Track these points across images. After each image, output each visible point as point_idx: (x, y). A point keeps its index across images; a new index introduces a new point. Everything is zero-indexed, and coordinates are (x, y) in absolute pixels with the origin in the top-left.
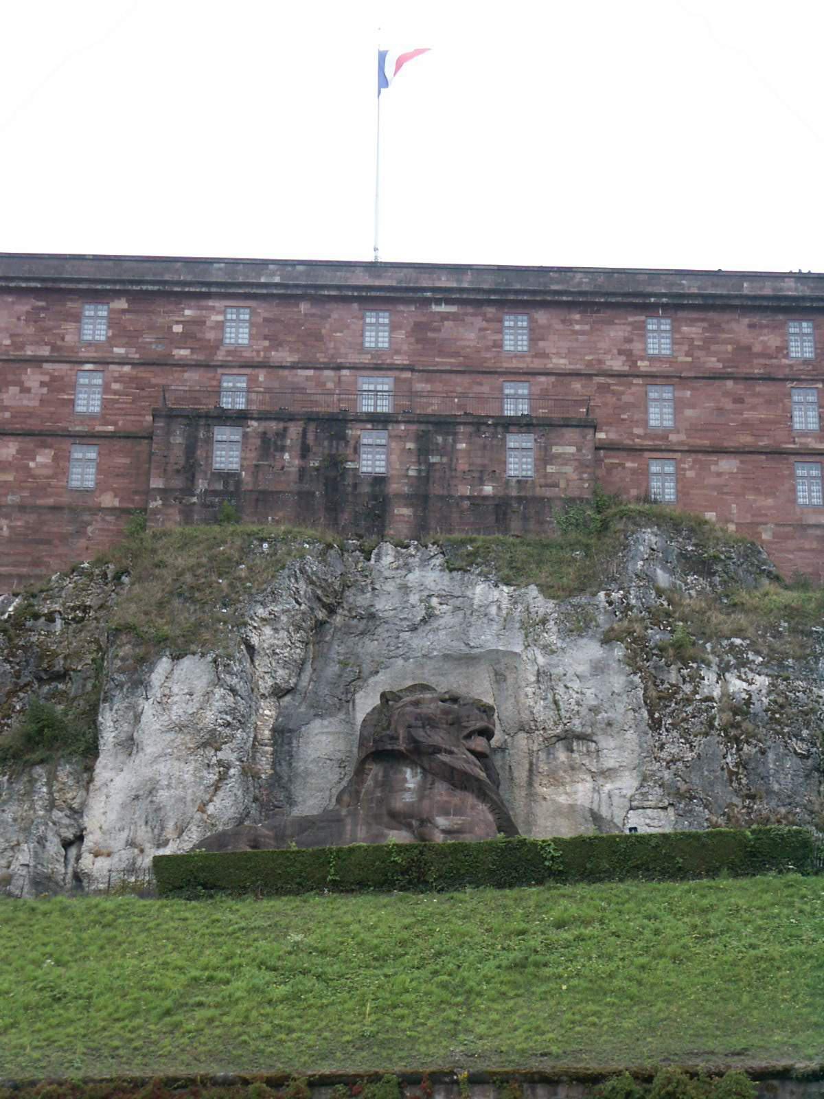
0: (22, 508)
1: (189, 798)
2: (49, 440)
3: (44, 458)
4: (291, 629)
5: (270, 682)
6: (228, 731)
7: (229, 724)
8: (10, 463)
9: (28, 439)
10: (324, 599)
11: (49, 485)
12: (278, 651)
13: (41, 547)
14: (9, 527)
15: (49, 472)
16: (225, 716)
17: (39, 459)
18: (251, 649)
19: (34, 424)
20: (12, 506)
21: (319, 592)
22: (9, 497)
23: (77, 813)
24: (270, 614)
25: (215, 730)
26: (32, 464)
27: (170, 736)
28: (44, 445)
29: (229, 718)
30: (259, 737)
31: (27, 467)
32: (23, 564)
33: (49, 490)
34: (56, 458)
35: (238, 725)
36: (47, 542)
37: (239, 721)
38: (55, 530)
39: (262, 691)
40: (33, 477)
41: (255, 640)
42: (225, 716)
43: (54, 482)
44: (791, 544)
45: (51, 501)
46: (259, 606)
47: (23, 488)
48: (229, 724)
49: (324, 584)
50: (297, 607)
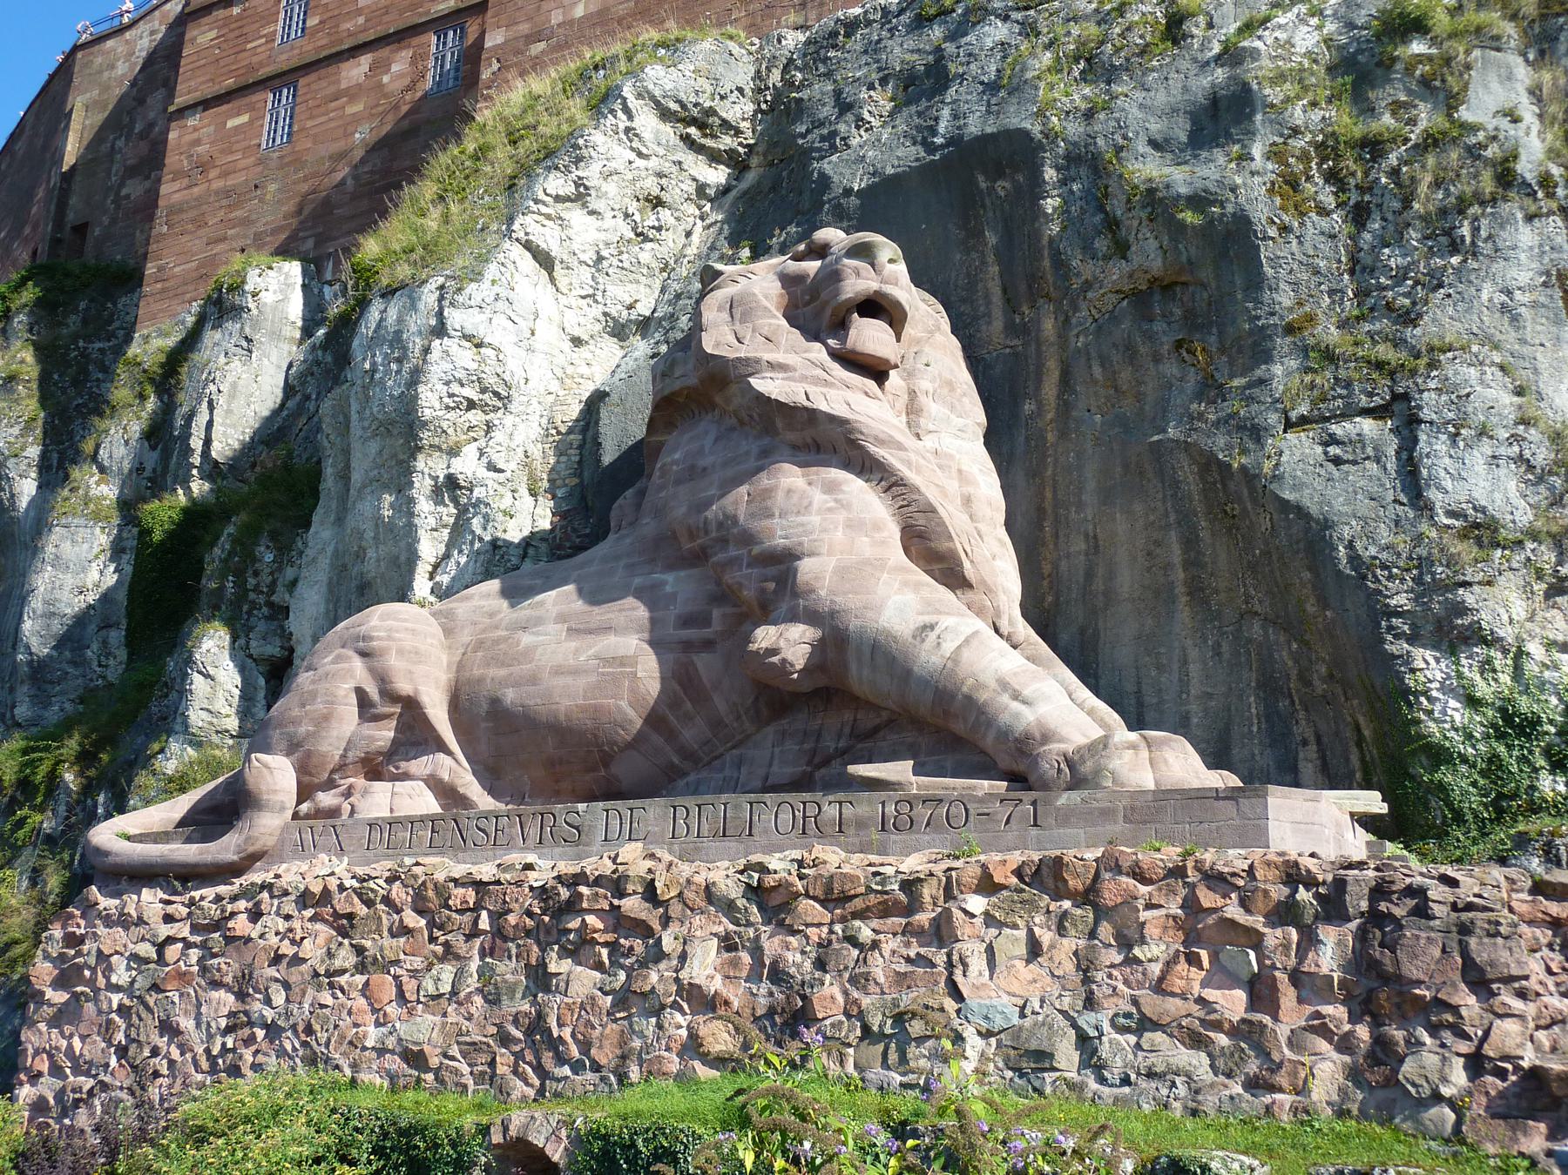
1: (403, 558)
4: (633, 207)
6: (475, 417)
7: (471, 405)
8: (359, 85)
10: (709, 142)
12: (605, 253)
15: (407, 81)
16: (455, 388)
17: (395, 68)
18: (544, 260)
24: (577, 185)
26: (386, 79)
27: (373, 447)
31: (381, 85)
34: (414, 61)
37: (497, 394)
40: (386, 96)
41: (547, 237)
42: (455, 388)
48: (471, 405)
49: (695, 112)
50: (640, 163)
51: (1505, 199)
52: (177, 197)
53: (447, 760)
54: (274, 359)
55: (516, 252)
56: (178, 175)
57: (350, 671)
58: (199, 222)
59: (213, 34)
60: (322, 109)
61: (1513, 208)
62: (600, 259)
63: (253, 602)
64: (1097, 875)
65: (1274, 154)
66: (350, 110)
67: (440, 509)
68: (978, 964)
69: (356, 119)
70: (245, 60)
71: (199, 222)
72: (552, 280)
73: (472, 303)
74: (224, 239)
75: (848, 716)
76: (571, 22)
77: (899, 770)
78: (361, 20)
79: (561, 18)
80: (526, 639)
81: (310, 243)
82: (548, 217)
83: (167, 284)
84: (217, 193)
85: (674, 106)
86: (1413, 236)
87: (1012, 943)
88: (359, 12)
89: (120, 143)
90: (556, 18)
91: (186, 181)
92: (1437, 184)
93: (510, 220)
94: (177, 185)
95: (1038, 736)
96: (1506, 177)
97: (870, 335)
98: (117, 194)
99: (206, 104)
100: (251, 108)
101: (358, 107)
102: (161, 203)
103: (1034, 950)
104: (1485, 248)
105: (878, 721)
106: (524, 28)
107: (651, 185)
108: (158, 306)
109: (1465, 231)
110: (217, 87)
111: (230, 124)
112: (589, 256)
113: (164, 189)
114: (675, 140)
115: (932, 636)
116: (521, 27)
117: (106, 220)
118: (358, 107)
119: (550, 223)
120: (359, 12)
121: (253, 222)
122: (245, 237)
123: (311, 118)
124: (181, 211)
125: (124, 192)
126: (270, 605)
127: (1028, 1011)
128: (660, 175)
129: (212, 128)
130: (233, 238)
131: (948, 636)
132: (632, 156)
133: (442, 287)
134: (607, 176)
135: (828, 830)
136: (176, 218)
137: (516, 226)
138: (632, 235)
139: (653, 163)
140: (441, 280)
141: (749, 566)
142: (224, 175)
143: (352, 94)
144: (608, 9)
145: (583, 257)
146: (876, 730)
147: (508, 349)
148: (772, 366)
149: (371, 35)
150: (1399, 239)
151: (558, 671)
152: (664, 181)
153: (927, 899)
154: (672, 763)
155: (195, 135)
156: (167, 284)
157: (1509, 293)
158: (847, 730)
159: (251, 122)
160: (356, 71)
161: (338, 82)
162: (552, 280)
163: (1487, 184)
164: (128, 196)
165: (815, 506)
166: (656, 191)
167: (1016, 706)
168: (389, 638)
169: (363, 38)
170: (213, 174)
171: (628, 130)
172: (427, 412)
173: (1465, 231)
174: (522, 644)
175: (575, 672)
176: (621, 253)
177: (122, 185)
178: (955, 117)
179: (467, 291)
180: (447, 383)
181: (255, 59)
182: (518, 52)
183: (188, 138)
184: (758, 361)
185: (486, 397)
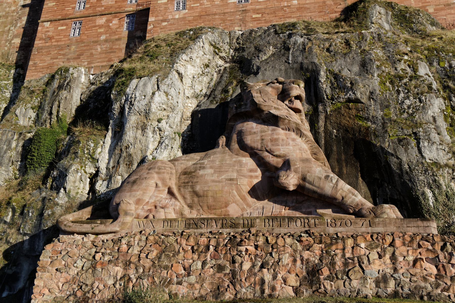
0: (106, 41)
2: (118, 15)
3: (115, 21)
5: (192, 91)
6: (165, 113)
9: (110, 15)
11: (117, 31)
12: (195, 77)
13: (112, 54)
14: (101, 48)
15: (118, 26)
17: (114, 22)
19: (113, 10)
20: (103, 40)
21: (216, 50)
22: (101, 37)
23: (95, 160)
25: (157, 112)
26: (111, 24)
28: (115, 17)
29: (164, 106)
30: (184, 117)
31: (109, 26)
32: (104, 62)
33: (116, 33)
35: (170, 110)
36: (115, 52)
38: (118, 47)
39: (188, 95)
40: (111, 29)
41: (182, 70)
43: (118, 30)
44: (443, 13)
45: (117, 37)
46: (184, 55)
47: (106, 34)
49: (218, 46)
50: (205, 56)
51: (432, 93)
52: (41, 45)
53: (178, 204)
54: (77, 92)
55: (175, 72)
56: (41, 39)
57: (153, 178)
58: (49, 53)
59: (54, 4)
60: (90, 29)
61: (433, 95)
62: (194, 78)
63: (86, 157)
64: (393, 240)
65: (378, 76)
66: (99, 31)
67: (155, 136)
68: (366, 261)
69: (101, 34)
70: (64, 12)
71: (49, 53)
72: (182, 80)
73: (166, 83)
74: (57, 58)
75: (294, 197)
76: (175, 19)
77: (329, 211)
78: (103, 8)
79: (172, 18)
80: (201, 172)
81: (86, 63)
82: (182, 65)
83: (37, 68)
84: (55, 45)
85: (213, 43)
86: (411, 98)
87: (374, 255)
88: (103, 6)
89: (12, 28)
90: (170, 17)
91: (43, 42)
92: (415, 87)
93: (173, 64)
94: (41, 42)
95: (360, 204)
96: (430, 87)
97: (298, 104)
98: (11, 42)
99: (51, 21)
100: (66, 25)
101: (102, 30)
102: (35, 46)
103: (380, 257)
104: (428, 103)
105: (304, 199)
106: (161, 18)
107: (206, 61)
108: (33, 74)
109: (423, 98)
110: (55, 18)
111: (59, 28)
112: (191, 77)
113: (36, 42)
114: (212, 52)
115: (329, 179)
116: (160, 18)
117: (6, 48)
118: (102, 30)
119: (182, 66)
120: (103, 6)
121: (67, 55)
122: (64, 58)
123: (87, 31)
124: (42, 49)
125: (13, 42)
126: (93, 159)
127: (380, 273)
128: (209, 60)
129: (53, 28)
130: (61, 58)
131: (333, 179)
132: (203, 53)
133: (157, 78)
134: (197, 57)
135: (312, 226)
136: (41, 51)
137: (175, 66)
138: (201, 73)
139: (208, 56)
140: (157, 76)
141: (272, 158)
142: (58, 41)
143: (100, 27)
144: (186, 17)
145: (190, 77)
146: (303, 201)
147: (174, 97)
148: (275, 108)
149: (107, 12)
150: (408, 98)
151: (213, 181)
152: (209, 61)
153: (349, 244)
154: (244, 208)
155: (48, 29)
156: (37, 68)
157: (434, 113)
158: (295, 201)
159: (66, 29)
160: (102, 21)
161: (95, 23)
162: (182, 80)
163: (426, 89)
164: (14, 43)
165: (291, 144)
166: (207, 63)
167: (354, 197)
168: (165, 169)
169: (104, 13)
170: (53, 40)
171: (203, 47)
172: (153, 110)
173: (423, 98)
174: (200, 174)
175: (219, 182)
176: (199, 77)
177: (12, 39)
178: (293, 57)
179: (165, 80)
180: (159, 104)
181: (68, 13)
182: (158, 24)
183: (44, 30)
184: (272, 106)
185: (168, 108)
